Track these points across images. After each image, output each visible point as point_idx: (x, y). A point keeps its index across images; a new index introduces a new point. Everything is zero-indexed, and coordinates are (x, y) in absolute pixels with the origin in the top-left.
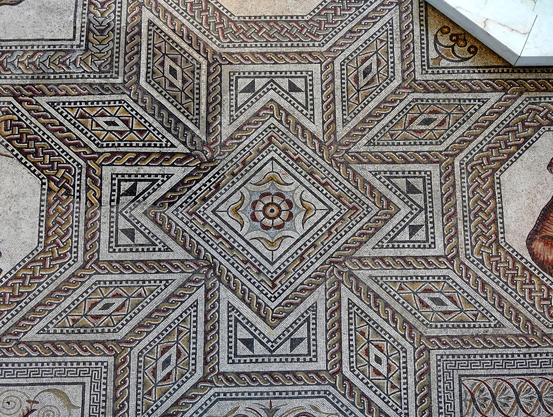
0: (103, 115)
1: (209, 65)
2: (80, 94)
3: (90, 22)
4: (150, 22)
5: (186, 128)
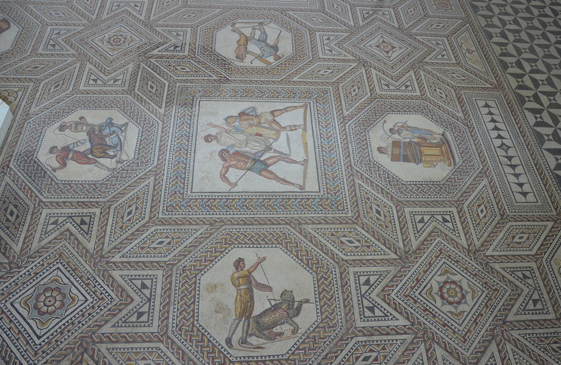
0: (187, 72)
1: (134, 90)
2: (197, 80)
3: (192, 108)
4: (161, 107)
5: (149, 67)
